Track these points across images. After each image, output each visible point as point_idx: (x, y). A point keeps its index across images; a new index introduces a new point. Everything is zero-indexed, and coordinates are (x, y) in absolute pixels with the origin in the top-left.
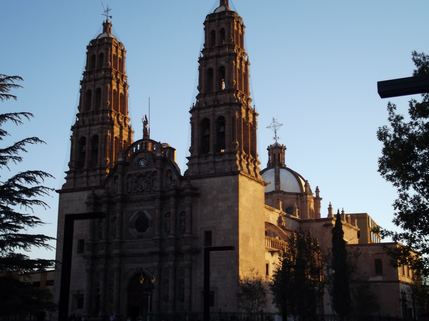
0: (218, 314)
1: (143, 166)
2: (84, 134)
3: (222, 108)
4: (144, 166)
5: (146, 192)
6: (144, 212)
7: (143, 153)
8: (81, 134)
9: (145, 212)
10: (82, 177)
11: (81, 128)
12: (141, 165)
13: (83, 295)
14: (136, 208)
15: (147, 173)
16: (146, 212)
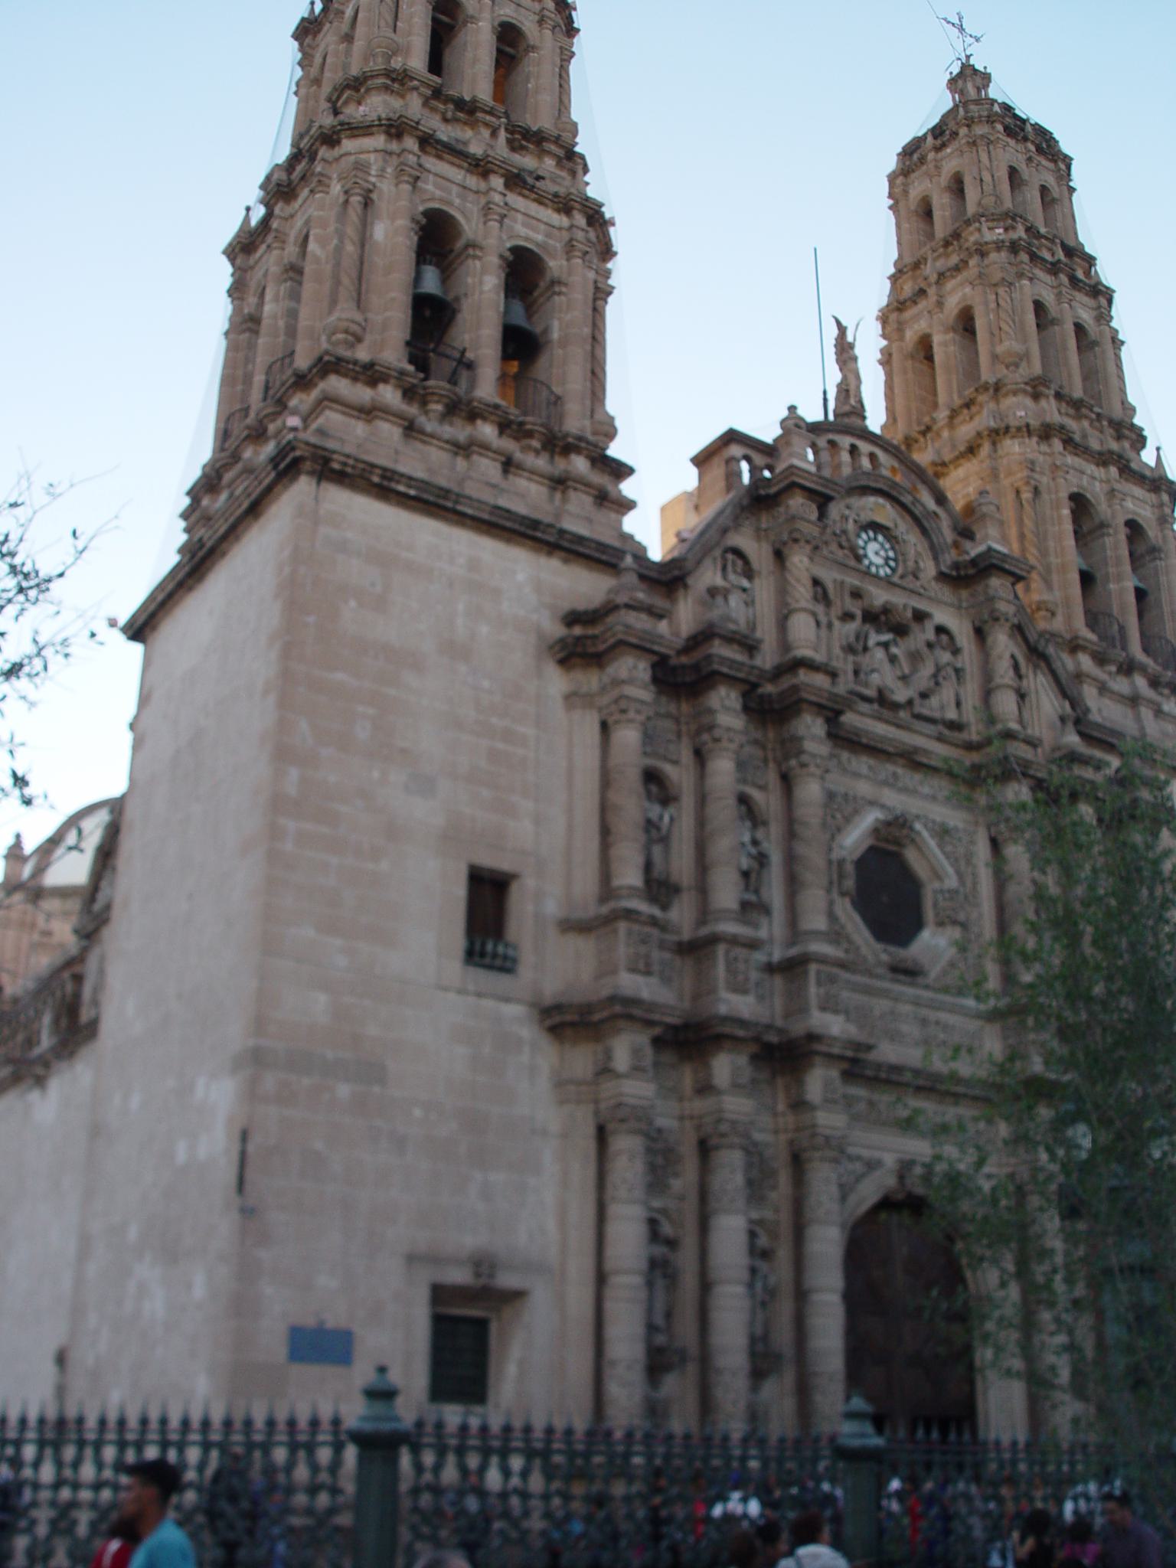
0: (351, 1453)
1: (877, 567)
2: (457, 201)
3: (1138, 491)
4: (887, 576)
5: (918, 717)
6: (918, 826)
7: (888, 506)
8: (430, 187)
9: (918, 833)
10: (464, 449)
11: (439, 157)
12: (865, 556)
13: (517, 1296)
14: (863, 788)
15: (920, 616)
16: (925, 834)
